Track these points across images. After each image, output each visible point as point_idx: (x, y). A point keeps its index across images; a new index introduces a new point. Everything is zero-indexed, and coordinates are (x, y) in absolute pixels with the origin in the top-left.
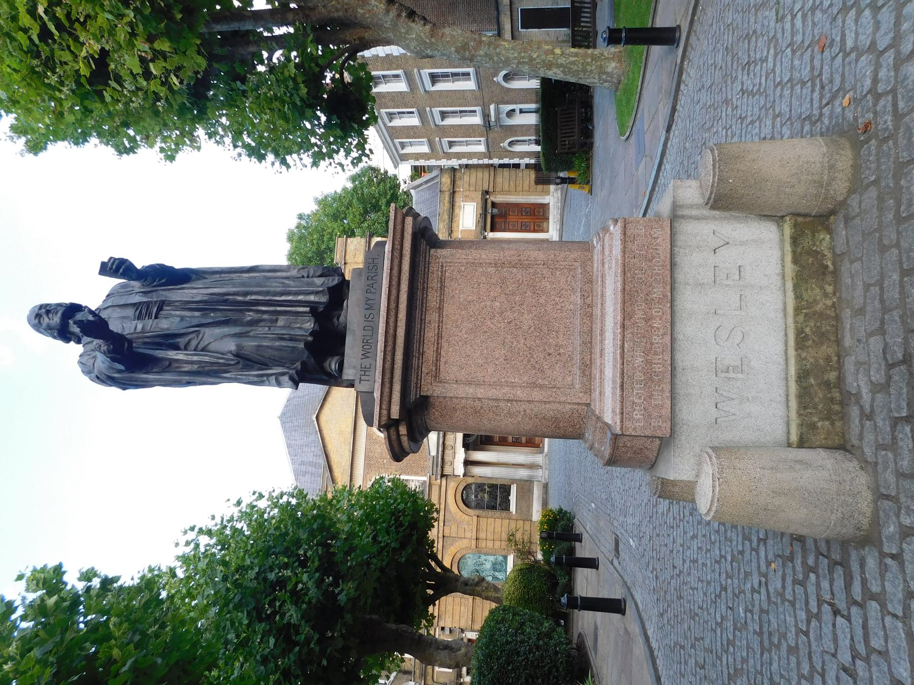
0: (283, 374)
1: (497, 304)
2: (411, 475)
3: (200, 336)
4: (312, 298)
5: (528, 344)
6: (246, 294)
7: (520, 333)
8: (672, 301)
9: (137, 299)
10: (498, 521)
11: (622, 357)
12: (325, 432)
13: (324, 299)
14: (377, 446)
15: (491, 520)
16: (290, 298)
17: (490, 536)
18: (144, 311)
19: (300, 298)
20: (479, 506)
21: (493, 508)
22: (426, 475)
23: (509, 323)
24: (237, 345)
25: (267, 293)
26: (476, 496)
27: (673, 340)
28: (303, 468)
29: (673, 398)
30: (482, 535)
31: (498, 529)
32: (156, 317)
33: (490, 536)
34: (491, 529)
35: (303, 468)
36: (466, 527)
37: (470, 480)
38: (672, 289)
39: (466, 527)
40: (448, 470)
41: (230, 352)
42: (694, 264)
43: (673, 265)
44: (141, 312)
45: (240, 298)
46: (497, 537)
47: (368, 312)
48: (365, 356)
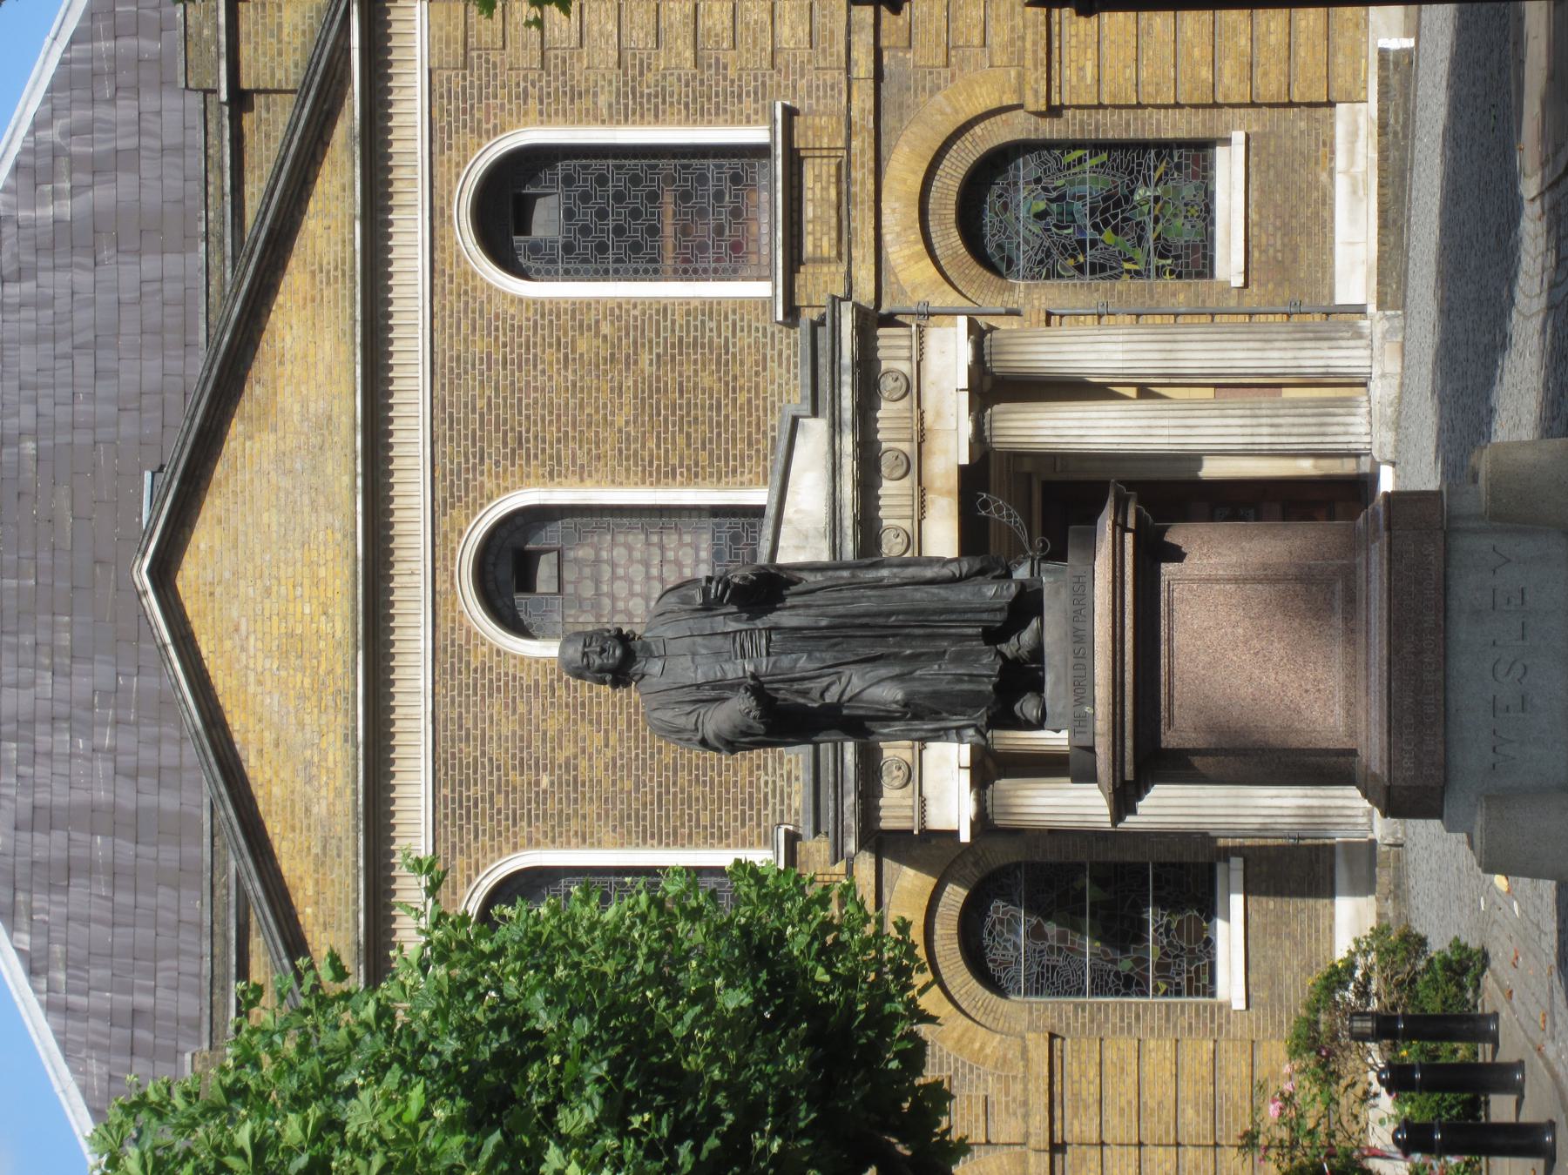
0: (968, 726)
1: (1240, 631)
2: (688, 841)
3: (844, 680)
4: (985, 616)
5: (1281, 678)
6: (890, 614)
7: (1270, 666)
8: (1445, 631)
9: (733, 626)
10: (1159, 1052)
11: (1389, 698)
12: (205, 646)
13: (1000, 617)
14: (496, 705)
15: (1120, 1049)
16: (954, 617)
17: (1119, 1127)
18: (747, 645)
19: (969, 616)
20: (1048, 981)
21: (1131, 984)
22: (767, 841)
23: (1256, 654)
24: (906, 694)
25: (923, 612)
26: (1036, 933)
27: (1446, 677)
28: (49, 845)
29: (1446, 743)
30: (1079, 1127)
31: (1158, 1091)
32: (768, 654)
33: (1119, 1127)
34: (1121, 1092)
35: (49, 845)
36: (992, 1087)
37: (1002, 854)
38: (1445, 617)
39: (992, 1087)
40: (895, 809)
41: (896, 702)
42: (1468, 588)
43: (1446, 588)
44: (742, 646)
45: (881, 621)
46: (1155, 1128)
47: (1078, 646)
48: (1079, 702)
